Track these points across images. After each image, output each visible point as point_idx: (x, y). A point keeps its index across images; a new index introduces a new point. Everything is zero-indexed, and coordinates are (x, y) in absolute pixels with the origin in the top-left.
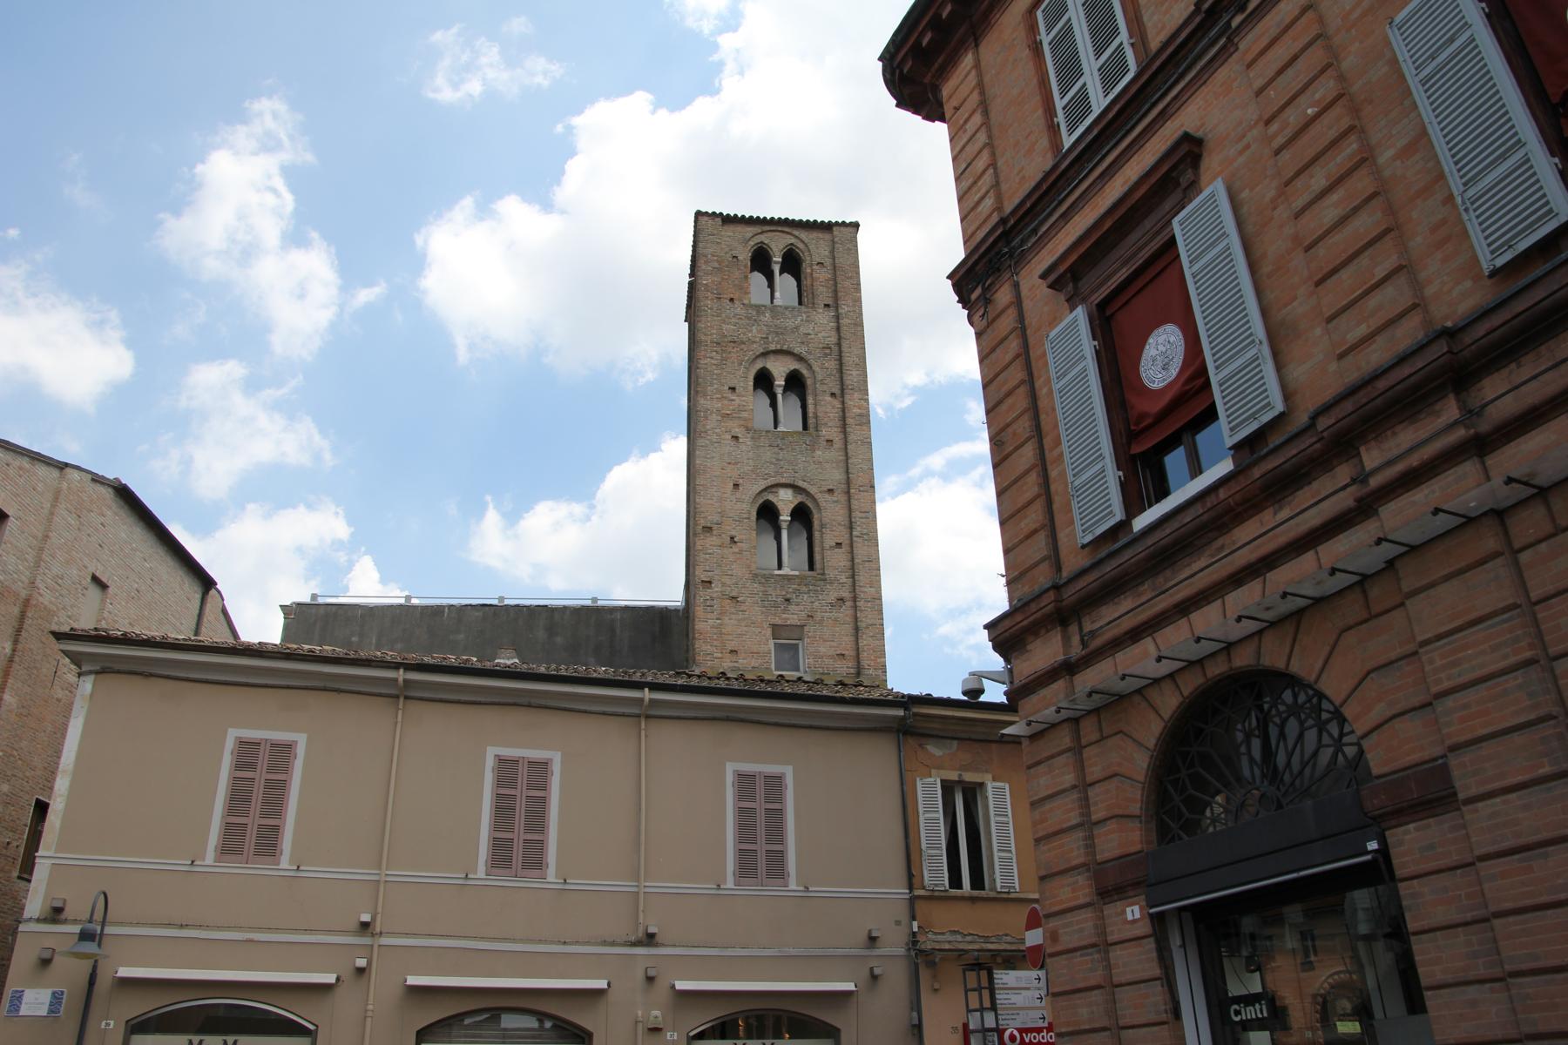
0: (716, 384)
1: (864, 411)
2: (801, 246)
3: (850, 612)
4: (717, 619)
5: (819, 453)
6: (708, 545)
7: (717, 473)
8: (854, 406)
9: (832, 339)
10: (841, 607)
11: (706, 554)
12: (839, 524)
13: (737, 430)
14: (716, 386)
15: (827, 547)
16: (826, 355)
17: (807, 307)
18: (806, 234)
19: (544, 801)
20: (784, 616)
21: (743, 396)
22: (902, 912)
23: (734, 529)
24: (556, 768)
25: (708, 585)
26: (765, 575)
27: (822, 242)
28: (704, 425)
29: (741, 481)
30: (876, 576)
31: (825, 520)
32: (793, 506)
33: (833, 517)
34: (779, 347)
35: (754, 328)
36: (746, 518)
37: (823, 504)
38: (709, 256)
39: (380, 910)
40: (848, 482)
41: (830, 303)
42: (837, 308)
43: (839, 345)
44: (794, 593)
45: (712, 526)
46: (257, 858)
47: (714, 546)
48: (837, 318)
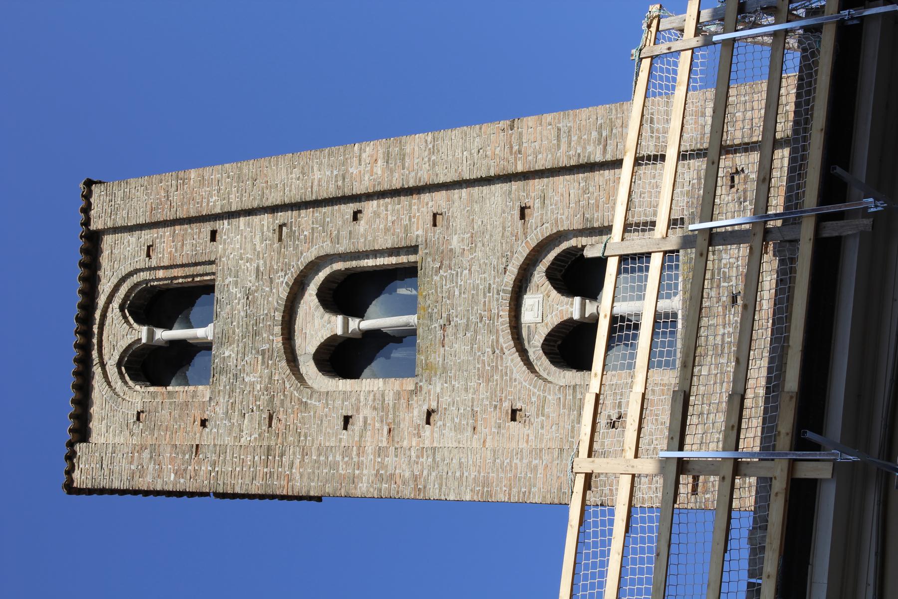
5: (455, 243)
12: (585, 191)
13: (416, 412)
14: (338, 458)
16: (291, 234)
21: (358, 400)
29: (507, 405)
32: (554, 293)
34: (278, 329)
37: (548, 230)
43: (273, 209)
44: (719, 286)
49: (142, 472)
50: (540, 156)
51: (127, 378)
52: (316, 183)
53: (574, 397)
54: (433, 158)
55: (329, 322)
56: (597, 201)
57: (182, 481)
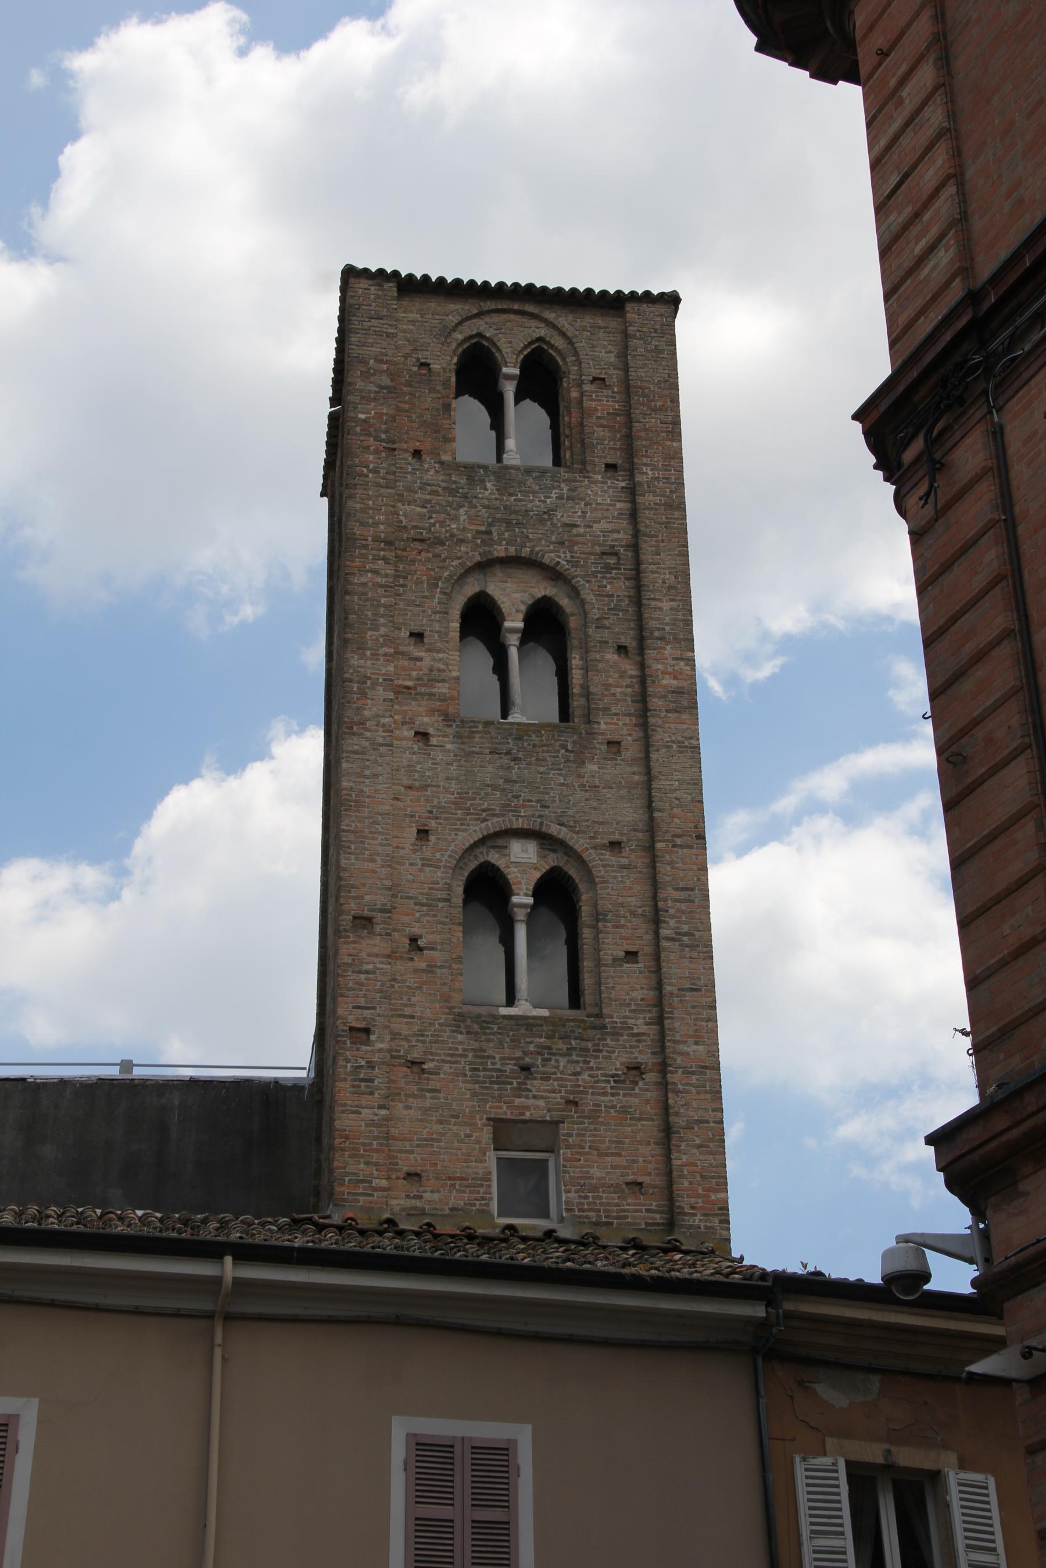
0: (384, 625)
1: (685, 684)
2: (559, 342)
3: (653, 1094)
4: (380, 1107)
6: (364, 955)
7: (386, 808)
8: (664, 673)
9: (621, 536)
10: (636, 1083)
11: (360, 972)
12: (633, 914)
13: (426, 719)
16: (608, 568)
17: (570, 469)
18: (570, 317)
20: (518, 1101)
21: (439, 651)
23: (418, 921)
25: (363, 1036)
26: (479, 1016)
27: (601, 334)
28: (358, 709)
29: (433, 824)
30: (709, 1020)
31: (605, 905)
32: (537, 875)
33: (621, 900)
34: (512, 551)
35: (462, 511)
36: (440, 900)
37: (599, 872)
38: (372, 362)
40: (651, 828)
41: (619, 462)
42: (632, 472)
43: (635, 547)
44: (539, 1053)
45: (373, 914)
47: (377, 956)
48: (632, 492)
49: (366, 375)
50: (668, 868)
51: (465, 346)
52: (659, 604)
53: (440, 900)
54: (675, 746)
55: (518, 611)
56: (623, 926)
57: (358, 429)
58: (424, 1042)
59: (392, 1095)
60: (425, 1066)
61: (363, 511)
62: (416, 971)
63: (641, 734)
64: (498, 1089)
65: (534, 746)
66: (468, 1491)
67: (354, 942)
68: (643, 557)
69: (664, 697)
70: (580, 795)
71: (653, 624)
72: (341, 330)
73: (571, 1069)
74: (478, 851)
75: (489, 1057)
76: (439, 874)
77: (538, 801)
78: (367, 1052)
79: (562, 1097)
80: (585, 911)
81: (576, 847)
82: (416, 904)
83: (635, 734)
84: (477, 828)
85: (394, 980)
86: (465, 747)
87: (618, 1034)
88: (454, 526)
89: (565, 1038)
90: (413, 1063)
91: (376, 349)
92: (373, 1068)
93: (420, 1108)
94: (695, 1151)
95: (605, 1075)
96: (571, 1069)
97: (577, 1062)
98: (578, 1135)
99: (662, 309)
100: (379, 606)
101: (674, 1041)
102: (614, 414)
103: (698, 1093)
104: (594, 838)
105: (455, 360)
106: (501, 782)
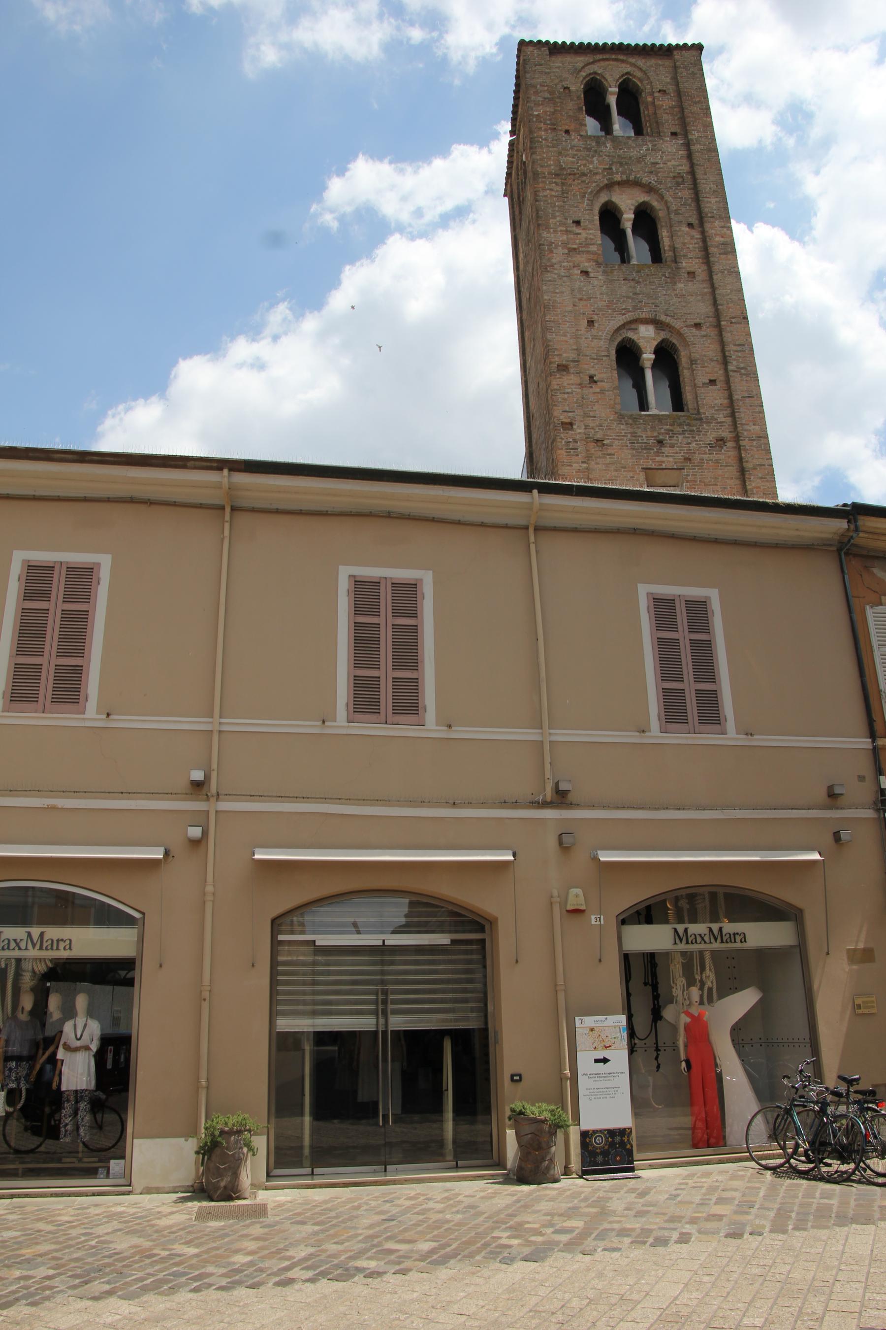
0: (559, 216)
1: (728, 240)
2: (639, 74)
3: (733, 453)
4: (583, 462)
5: (680, 285)
6: (565, 384)
7: (570, 309)
8: (715, 235)
9: (683, 167)
10: (722, 448)
11: (564, 393)
12: (712, 360)
13: (586, 264)
14: (558, 219)
15: (700, 384)
16: (678, 184)
17: (652, 136)
18: (643, 61)
19: (414, 631)
20: (658, 459)
21: (590, 229)
22: (865, 766)
23: (593, 367)
24: (428, 590)
25: (569, 427)
26: (632, 415)
27: (661, 68)
28: (549, 259)
29: (595, 318)
30: (760, 412)
31: (696, 356)
32: (655, 343)
33: (704, 353)
34: (624, 177)
35: (595, 159)
36: (604, 356)
37: (690, 339)
38: (538, 86)
39: (214, 766)
40: (717, 315)
41: (678, 131)
42: (686, 135)
43: (692, 173)
45: (569, 363)
46: (56, 706)
47: (573, 384)
48: (688, 145)
49: (536, 93)
50: (729, 334)
51: (587, 79)
52: (709, 200)
53: (604, 356)
54: (726, 272)
55: (630, 209)
56: (706, 367)
57: (535, 120)
58: (602, 430)
59: (588, 458)
60: (605, 442)
61: (541, 160)
62: (594, 393)
63: (706, 268)
64: (647, 453)
65: (647, 275)
66: (686, 624)
67: (559, 378)
68: (697, 176)
69: (717, 247)
70: (675, 300)
71: (706, 210)
72: (517, 85)
73: (685, 441)
74: (621, 332)
75: (639, 436)
76: (602, 343)
77: (653, 303)
78: (572, 434)
79: (682, 456)
80: (684, 361)
81: (676, 326)
82: (591, 359)
83: (702, 268)
84: (620, 319)
85: (583, 398)
86: (610, 277)
87: (710, 422)
88: (591, 166)
89: (680, 425)
90: (597, 440)
91: (540, 80)
92: (577, 442)
93: (604, 464)
94: (758, 480)
95: (705, 444)
96: (685, 441)
97: (689, 437)
98: (692, 475)
99: (694, 53)
100: (555, 206)
101: (742, 424)
102: (672, 108)
103: (758, 450)
104: (686, 321)
105: (582, 87)
106: (631, 294)
